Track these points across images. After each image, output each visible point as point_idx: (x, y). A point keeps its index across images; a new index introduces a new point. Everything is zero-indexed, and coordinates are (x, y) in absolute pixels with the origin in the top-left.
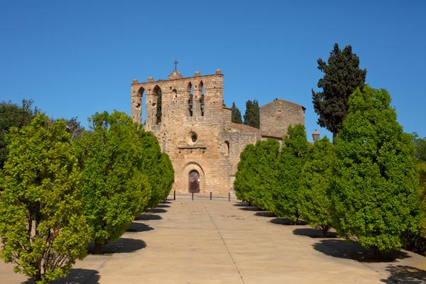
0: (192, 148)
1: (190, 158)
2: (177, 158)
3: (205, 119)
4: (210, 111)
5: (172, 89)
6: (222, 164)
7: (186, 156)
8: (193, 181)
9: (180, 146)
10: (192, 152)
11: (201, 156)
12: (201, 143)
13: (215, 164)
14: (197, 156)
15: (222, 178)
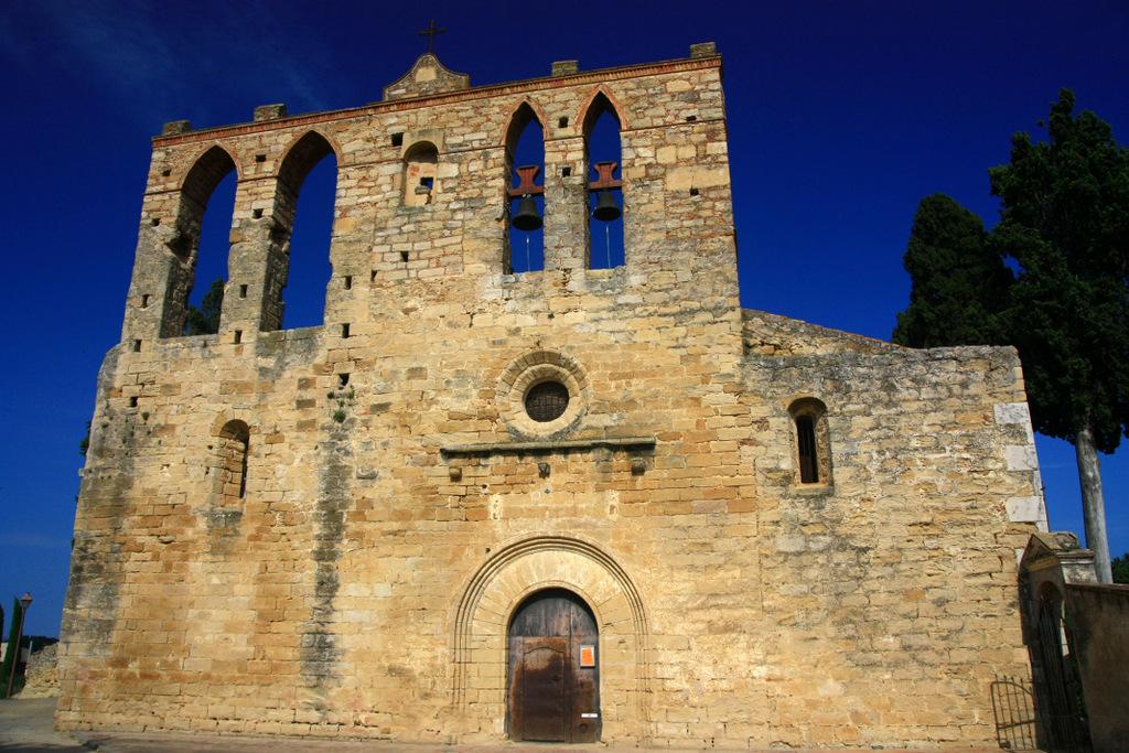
1: (531, 513)
2: (426, 515)
3: (635, 280)
5: (408, 142)
6: (784, 543)
7: (496, 503)
9: (450, 443)
10: (545, 474)
11: (613, 497)
13: (722, 545)
14: (587, 500)
15: (787, 634)
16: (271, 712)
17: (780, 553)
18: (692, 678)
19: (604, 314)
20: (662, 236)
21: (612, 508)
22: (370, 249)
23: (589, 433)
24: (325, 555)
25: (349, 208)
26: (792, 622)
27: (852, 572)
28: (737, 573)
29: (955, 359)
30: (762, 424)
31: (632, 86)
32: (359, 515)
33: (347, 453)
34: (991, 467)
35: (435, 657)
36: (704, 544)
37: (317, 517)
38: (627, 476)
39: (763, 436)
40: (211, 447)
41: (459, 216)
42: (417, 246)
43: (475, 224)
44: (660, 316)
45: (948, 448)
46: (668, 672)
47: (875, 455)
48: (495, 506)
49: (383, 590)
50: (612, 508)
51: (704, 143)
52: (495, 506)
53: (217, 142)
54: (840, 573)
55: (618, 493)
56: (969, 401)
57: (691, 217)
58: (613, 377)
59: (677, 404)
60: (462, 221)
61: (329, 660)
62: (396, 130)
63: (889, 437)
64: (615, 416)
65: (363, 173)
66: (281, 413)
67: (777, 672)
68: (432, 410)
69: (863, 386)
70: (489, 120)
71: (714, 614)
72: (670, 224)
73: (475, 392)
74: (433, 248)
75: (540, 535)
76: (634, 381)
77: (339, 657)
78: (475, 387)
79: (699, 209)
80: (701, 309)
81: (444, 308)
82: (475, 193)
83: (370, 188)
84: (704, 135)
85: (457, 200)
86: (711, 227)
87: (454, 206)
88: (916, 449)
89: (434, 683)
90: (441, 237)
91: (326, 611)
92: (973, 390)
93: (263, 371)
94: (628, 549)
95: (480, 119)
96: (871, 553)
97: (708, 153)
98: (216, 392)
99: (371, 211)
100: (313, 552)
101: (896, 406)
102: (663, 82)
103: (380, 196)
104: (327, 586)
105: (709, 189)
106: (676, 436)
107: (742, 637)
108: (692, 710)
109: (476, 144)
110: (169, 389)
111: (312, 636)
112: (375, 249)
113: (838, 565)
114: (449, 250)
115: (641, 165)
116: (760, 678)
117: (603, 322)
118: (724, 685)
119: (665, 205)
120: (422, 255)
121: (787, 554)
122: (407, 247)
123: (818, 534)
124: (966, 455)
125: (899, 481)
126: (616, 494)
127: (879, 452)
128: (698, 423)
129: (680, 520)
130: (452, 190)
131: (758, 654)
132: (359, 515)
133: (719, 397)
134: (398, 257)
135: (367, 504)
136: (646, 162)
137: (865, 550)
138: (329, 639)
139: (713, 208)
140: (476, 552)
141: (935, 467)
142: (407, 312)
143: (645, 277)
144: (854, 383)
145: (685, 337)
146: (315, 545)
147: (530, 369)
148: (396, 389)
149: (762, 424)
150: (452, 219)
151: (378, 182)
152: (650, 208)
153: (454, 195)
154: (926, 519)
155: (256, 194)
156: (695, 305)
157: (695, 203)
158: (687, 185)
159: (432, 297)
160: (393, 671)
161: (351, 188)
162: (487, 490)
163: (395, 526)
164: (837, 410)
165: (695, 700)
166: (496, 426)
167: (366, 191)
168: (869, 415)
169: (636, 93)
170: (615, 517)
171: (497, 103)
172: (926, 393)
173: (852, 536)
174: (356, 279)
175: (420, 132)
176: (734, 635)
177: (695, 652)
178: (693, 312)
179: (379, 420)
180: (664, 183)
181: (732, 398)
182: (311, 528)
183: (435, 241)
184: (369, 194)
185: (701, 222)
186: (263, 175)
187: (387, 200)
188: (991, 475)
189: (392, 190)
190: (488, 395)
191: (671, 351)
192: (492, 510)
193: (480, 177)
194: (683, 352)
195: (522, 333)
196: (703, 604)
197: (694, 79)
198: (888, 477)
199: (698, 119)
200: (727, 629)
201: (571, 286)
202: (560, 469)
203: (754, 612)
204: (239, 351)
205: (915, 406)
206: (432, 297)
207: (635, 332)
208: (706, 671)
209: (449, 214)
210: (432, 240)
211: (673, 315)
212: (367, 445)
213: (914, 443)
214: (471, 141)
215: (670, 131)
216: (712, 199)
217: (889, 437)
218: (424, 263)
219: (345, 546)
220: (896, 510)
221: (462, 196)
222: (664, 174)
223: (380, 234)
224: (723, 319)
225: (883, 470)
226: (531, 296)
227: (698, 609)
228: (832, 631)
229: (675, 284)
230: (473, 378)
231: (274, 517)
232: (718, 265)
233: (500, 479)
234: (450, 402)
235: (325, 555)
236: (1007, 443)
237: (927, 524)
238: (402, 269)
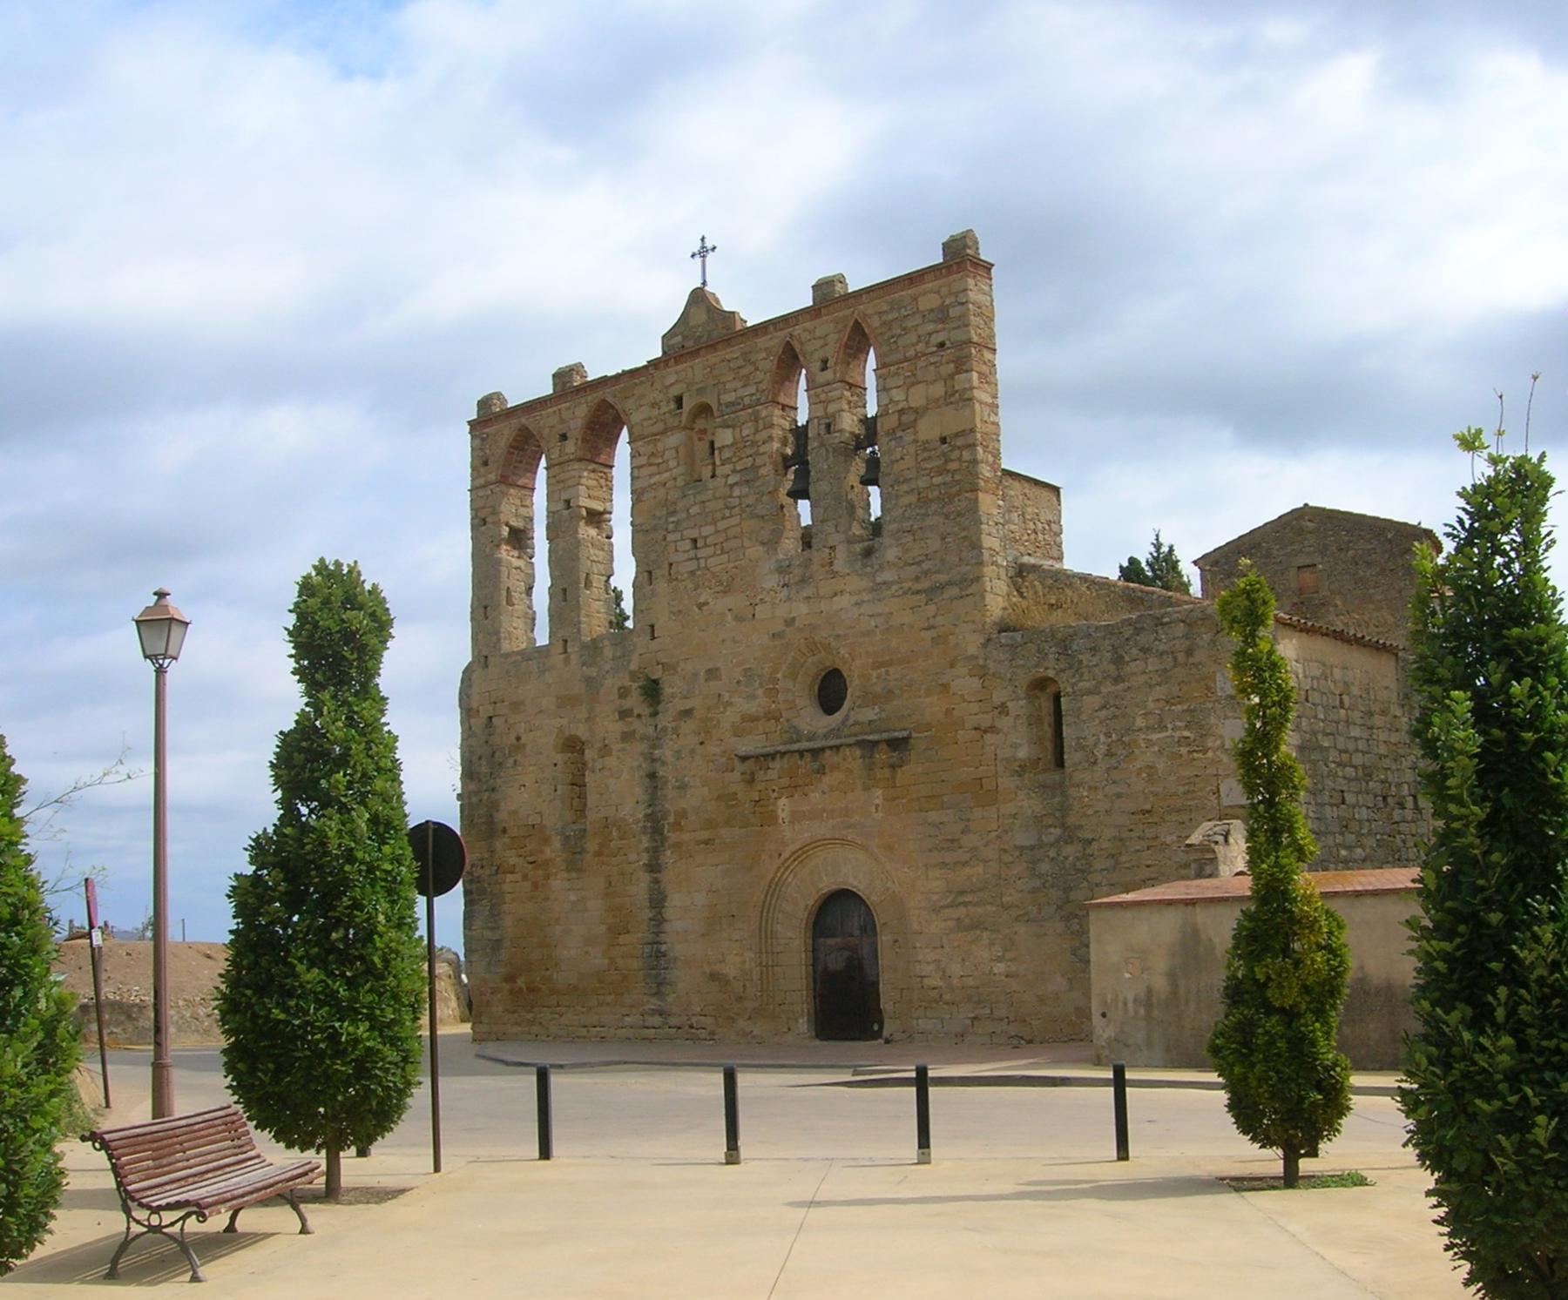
0: (816, 753)
3: (891, 554)
4: (923, 502)
6: (1023, 839)
7: (783, 807)
8: (836, 962)
9: (747, 746)
10: (821, 771)
12: (869, 714)
13: (969, 841)
15: (1021, 929)
16: (627, 1019)
17: (1016, 847)
18: (946, 977)
19: (865, 596)
20: (913, 498)
21: (877, 806)
23: (854, 729)
24: (654, 867)
26: (1026, 918)
27: (1079, 866)
28: (980, 869)
29: (1183, 622)
30: (1003, 709)
32: (677, 826)
33: (664, 763)
34: (1210, 745)
35: (744, 962)
36: (952, 841)
37: (644, 831)
38: (887, 773)
39: (1004, 723)
40: (556, 765)
43: (750, 500)
44: (913, 594)
45: (1170, 726)
46: (928, 969)
47: (1102, 738)
48: (783, 810)
49: (700, 899)
50: (877, 806)
51: (952, 376)
52: (783, 810)
53: (523, 420)
54: (1068, 866)
55: (881, 792)
56: (1194, 670)
57: (942, 471)
58: (877, 665)
59: (928, 693)
60: (739, 497)
61: (664, 969)
62: (675, 391)
63: (1115, 717)
64: (877, 709)
65: (650, 448)
66: (611, 727)
67: (1013, 968)
68: (728, 713)
69: (1095, 660)
70: (757, 369)
71: (962, 911)
72: (922, 483)
73: (760, 692)
74: (717, 532)
75: (819, 837)
76: (892, 670)
77: (672, 965)
78: (761, 685)
79: (946, 462)
80: (950, 583)
81: (729, 601)
82: (748, 462)
83: (658, 464)
84: (952, 365)
85: (734, 471)
86: (958, 482)
87: (731, 481)
88: (1140, 729)
89: (744, 986)
90: (723, 518)
91: (658, 921)
92: (1198, 656)
94: (890, 848)
96: (1095, 845)
97: (956, 388)
98: (553, 707)
100: (644, 864)
101: (1123, 681)
102: (915, 299)
103: (668, 474)
104: (658, 901)
105: (957, 435)
106: (929, 727)
107: (985, 935)
108: (945, 1006)
109: (747, 401)
110: (516, 706)
111: (650, 946)
112: (670, 537)
113: (1066, 858)
114: (731, 533)
115: (893, 413)
116: (1000, 974)
117: (865, 605)
118: (970, 982)
119: (916, 459)
120: (709, 541)
121: (1022, 849)
122: (694, 533)
123: (1050, 826)
124: (1186, 734)
125: (1123, 765)
126: (879, 792)
127: (1105, 734)
128: (948, 712)
129: (933, 816)
131: (997, 951)
132: (677, 826)
133: (964, 683)
134: (688, 545)
135: (682, 814)
136: (900, 406)
137: (1090, 842)
138: (664, 948)
139: (960, 459)
140: (771, 856)
141: (1156, 749)
142: (700, 606)
143: (900, 548)
144: (1085, 658)
145: (934, 617)
146: (645, 858)
147: (810, 660)
148: (697, 692)
149: (1003, 709)
150: (731, 497)
151: (666, 457)
152: (903, 465)
153: (731, 466)
154: (1148, 807)
155: (563, 481)
156: (943, 578)
157: (944, 454)
158: (935, 435)
159: (721, 588)
160: (714, 977)
161: (642, 466)
162: (775, 795)
163: (704, 835)
164: (1069, 690)
165: (947, 997)
166: (779, 727)
167: (653, 469)
168: (1099, 693)
169: (890, 317)
170: (880, 815)
172: (1153, 664)
173: (1080, 827)
174: (657, 573)
175: (698, 390)
176: (978, 932)
177: (947, 949)
178: (942, 587)
179: (687, 726)
180: (915, 433)
181: (975, 683)
182: (640, 841)
183: (718, 524)
184: (659, 473)
185: (949, 478)
186: (566, 458)
187: (675, 479)
188: (1210, 754)
189: (678, 465)
190: (772, 693)
191: (923, 634)
192: (781, 814)
193: (752, 442)
194: (933, 633)
195: (797, 623)
196: (953, 901)
197: (944, 290)
198: (1113, 761)
199: (948, 344)
200: (973, 927)
201: (839, 565)
202: (835, 767)
203: (994, 909)
204: (567, 661)
205: (1143, 678)
206: (721, 588)
207: (892, 613)
208: (955, 969)
209: (727, 489)
210: (715, 523)
211: (925, 591)
212: (678, 754)
213: (1140, 722)
214: (742, 398)
215: (921, 363)
216: (959, 448)
217: (1115, 717)
218: (710, 551)
219: (668, 856)
220: (1119, 796)
221: (738, 468)
222: (915, 420)
223: (672, 519)
224: (968, 592)
225: (1109, 754)
226: (803, 580)
227: (948, 906)
228: (1060, 926)
229: (927, 555)
230: (759, 676)
231: (611, 832)
232: (964, 529)
233: (785, 781)
234: (743, 706)
235: (654, 867)
236: (1226, 717)
237: (1148, 812)
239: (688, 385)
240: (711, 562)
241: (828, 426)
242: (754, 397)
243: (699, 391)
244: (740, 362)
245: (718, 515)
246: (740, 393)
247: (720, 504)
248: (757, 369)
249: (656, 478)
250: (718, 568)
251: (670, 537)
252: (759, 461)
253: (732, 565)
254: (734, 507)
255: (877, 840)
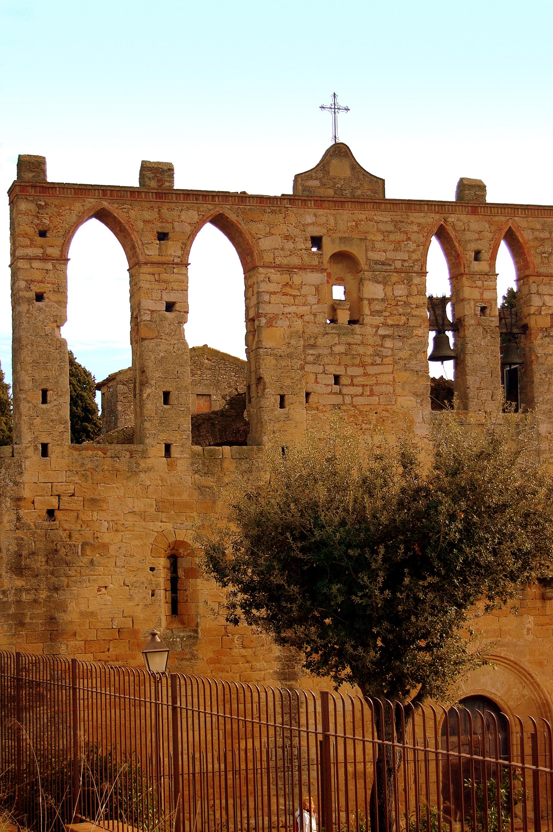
22: (302, 368)
25: (275, 317)
31: (538, 226)
41: (388, 343)
42: (352, 371)
43: (404, 354)
65: (285, 278)
70: (409, 239)
83: (295, 296)
85: (385, 324)
90: (372, 364)
93: (201, 488)
95: (399, 237)
99: (298, 324)
103: (307, 308)
109: (398, 264)
112: (308, 368)
115: (547, 315)
122: (340, 371)
130: (379, 313)
153: (382, 319)
161: (275, 293)
171: (416, 221)
175: (340, 238)
221: (390, 322)
223: (311, 352)
238: (335, 393)
239: (329, 230)
240: (358, 401)
241: (483, 309)
242: (406, 264)
243: (343, 240)
244: (391, 227)
245: (369, 360)
246: (390, 255)
247: (370, 351)
248: (409, 239)
249: (292, 309)
250: (368, 408)
251: (308, 368)
252: (412, 322)
253: (382, 407)
254: (386, 357)
255: (528, 657)
